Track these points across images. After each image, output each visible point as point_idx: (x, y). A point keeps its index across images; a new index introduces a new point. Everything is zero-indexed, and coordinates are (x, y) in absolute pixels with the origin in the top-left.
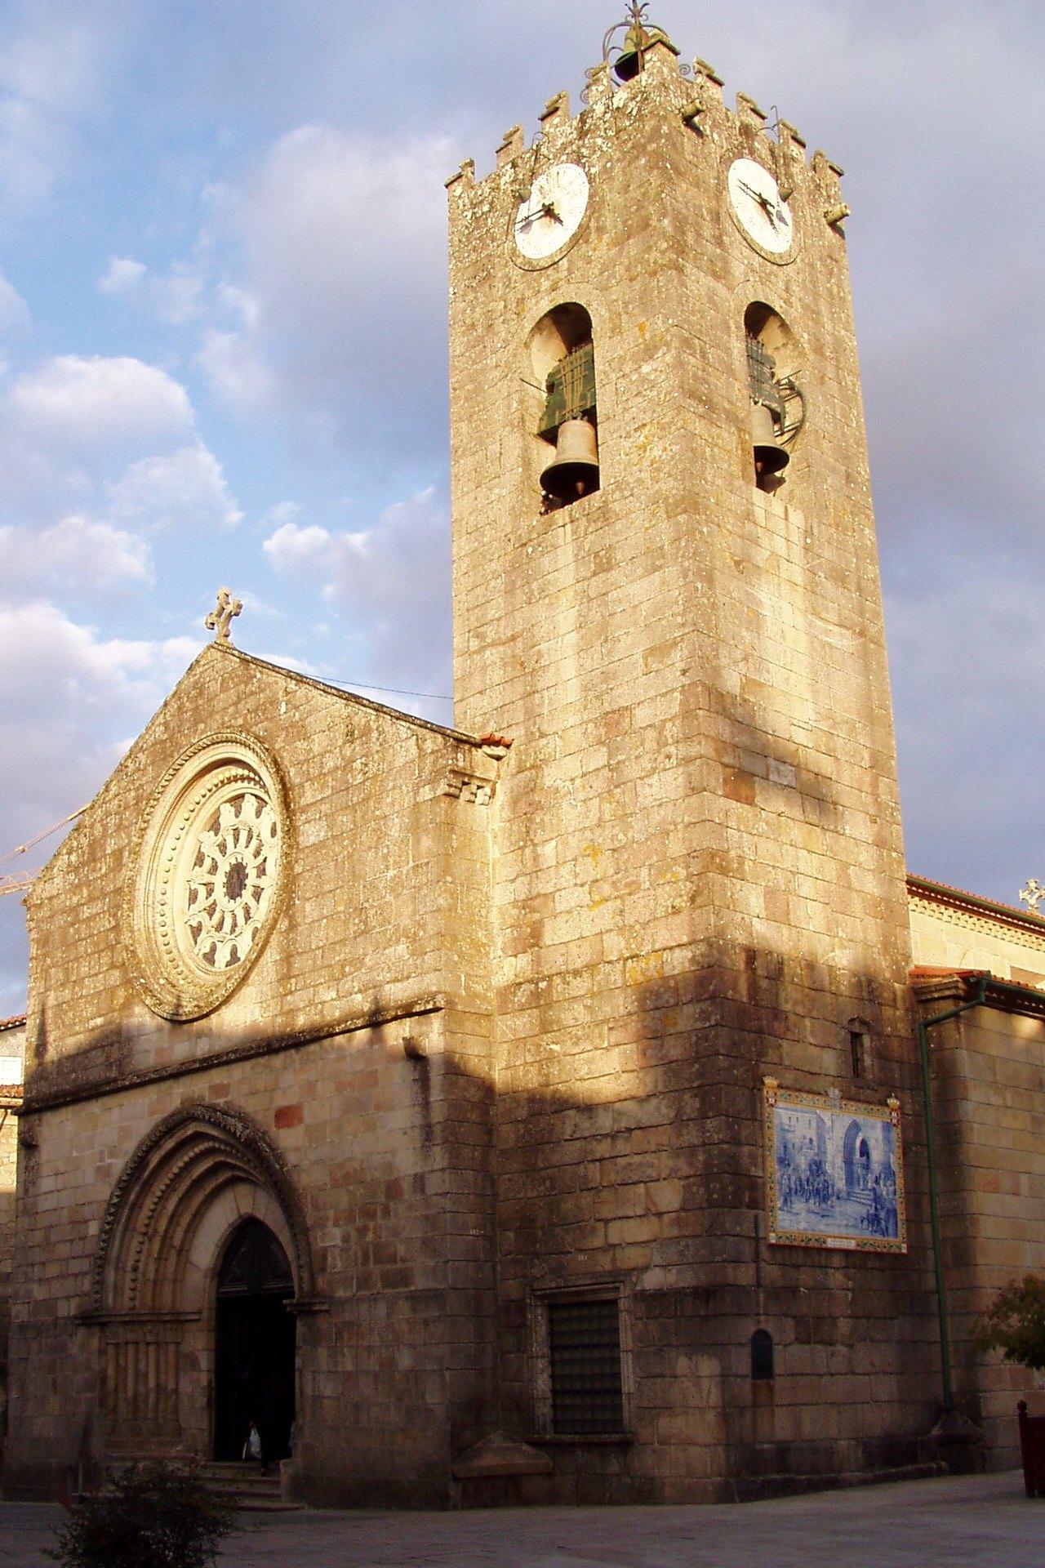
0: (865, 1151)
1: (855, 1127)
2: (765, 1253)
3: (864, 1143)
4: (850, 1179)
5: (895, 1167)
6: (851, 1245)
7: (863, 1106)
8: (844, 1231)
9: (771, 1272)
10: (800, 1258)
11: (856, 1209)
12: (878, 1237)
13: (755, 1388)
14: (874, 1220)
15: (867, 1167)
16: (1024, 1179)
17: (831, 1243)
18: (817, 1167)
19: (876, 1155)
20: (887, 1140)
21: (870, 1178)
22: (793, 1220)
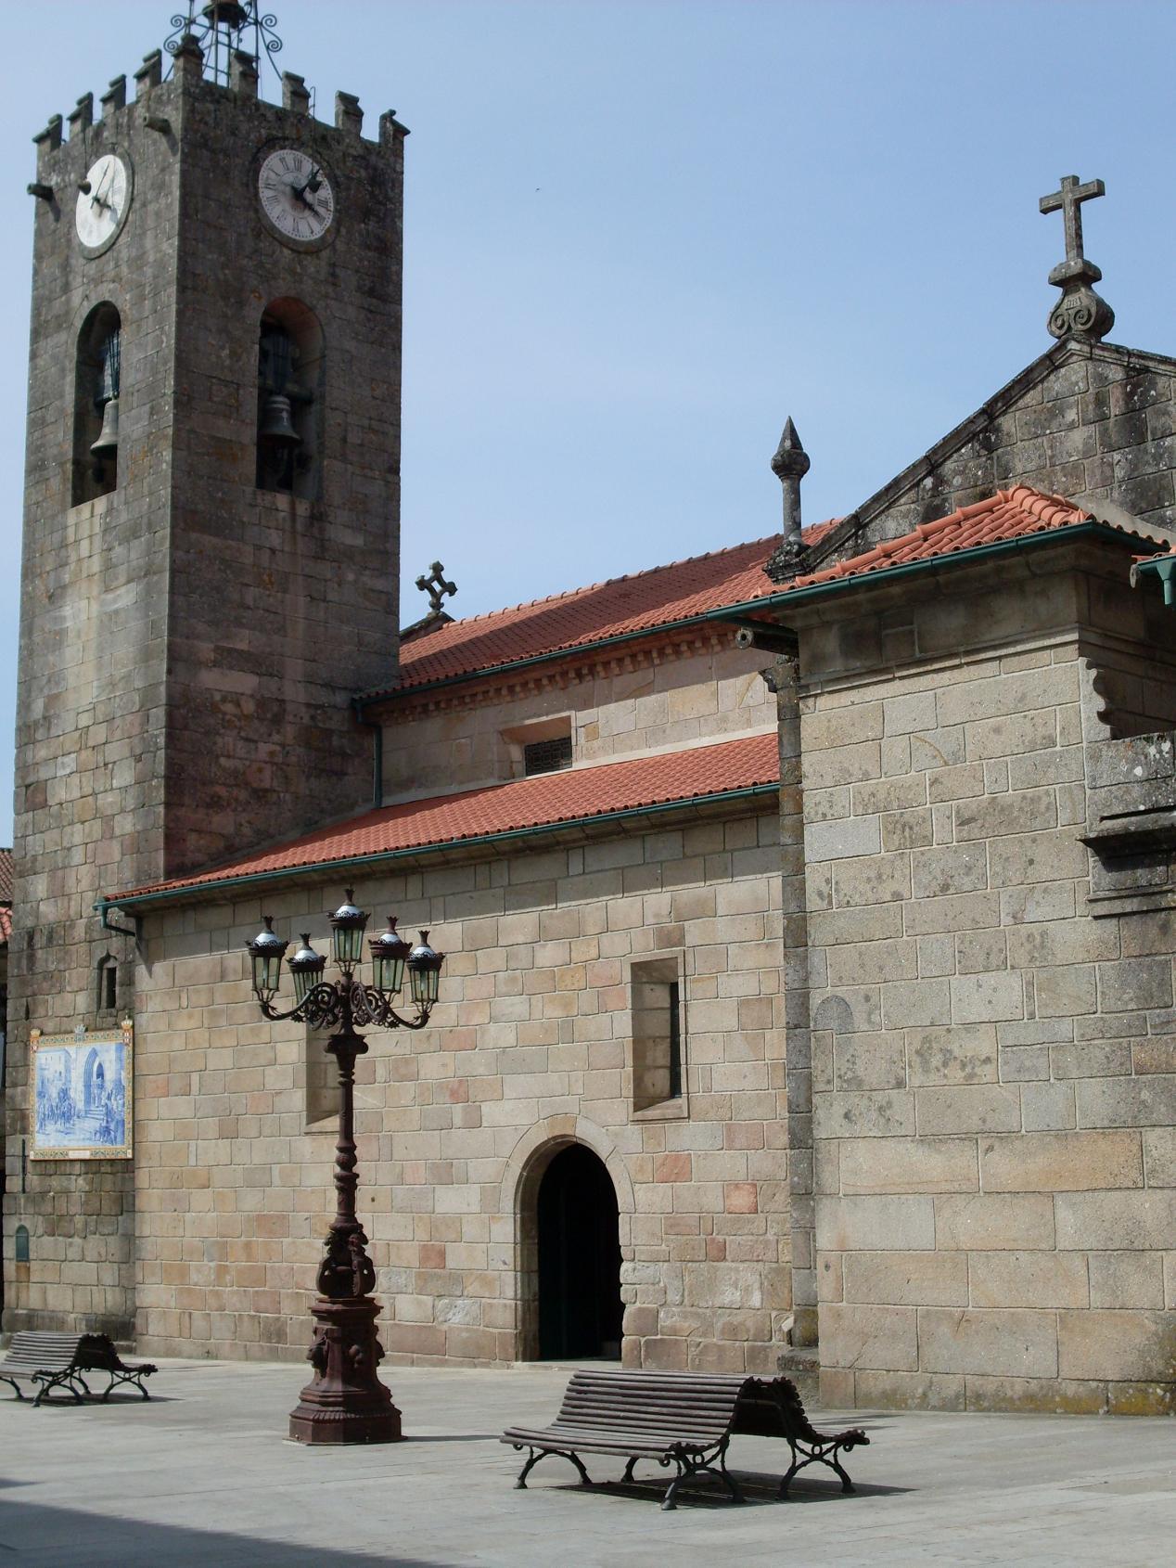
0: (101, 1075)
1: (94, 1053)
2: (29, 1166)
3: (100, 1066)
4: (88, 1102)
5: (125, 1083)
6: (86, 1155)
7: (100, 1034)
8: (81, 1144)
9: (34, 1181)
10: (51, 1168)
11: (93, 1124)
12: (108, 1145)
13: (18, 1268)
14: (107, 1130)
15: (102, 1087)
16: (195, 1077)
17: (72, 1155)
18: (64, 1094)
19: (110, 1075)
20: (120, 1059)
21: (104, 1095)
22: (46, 1140)
